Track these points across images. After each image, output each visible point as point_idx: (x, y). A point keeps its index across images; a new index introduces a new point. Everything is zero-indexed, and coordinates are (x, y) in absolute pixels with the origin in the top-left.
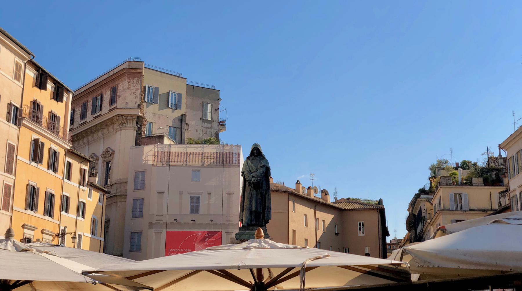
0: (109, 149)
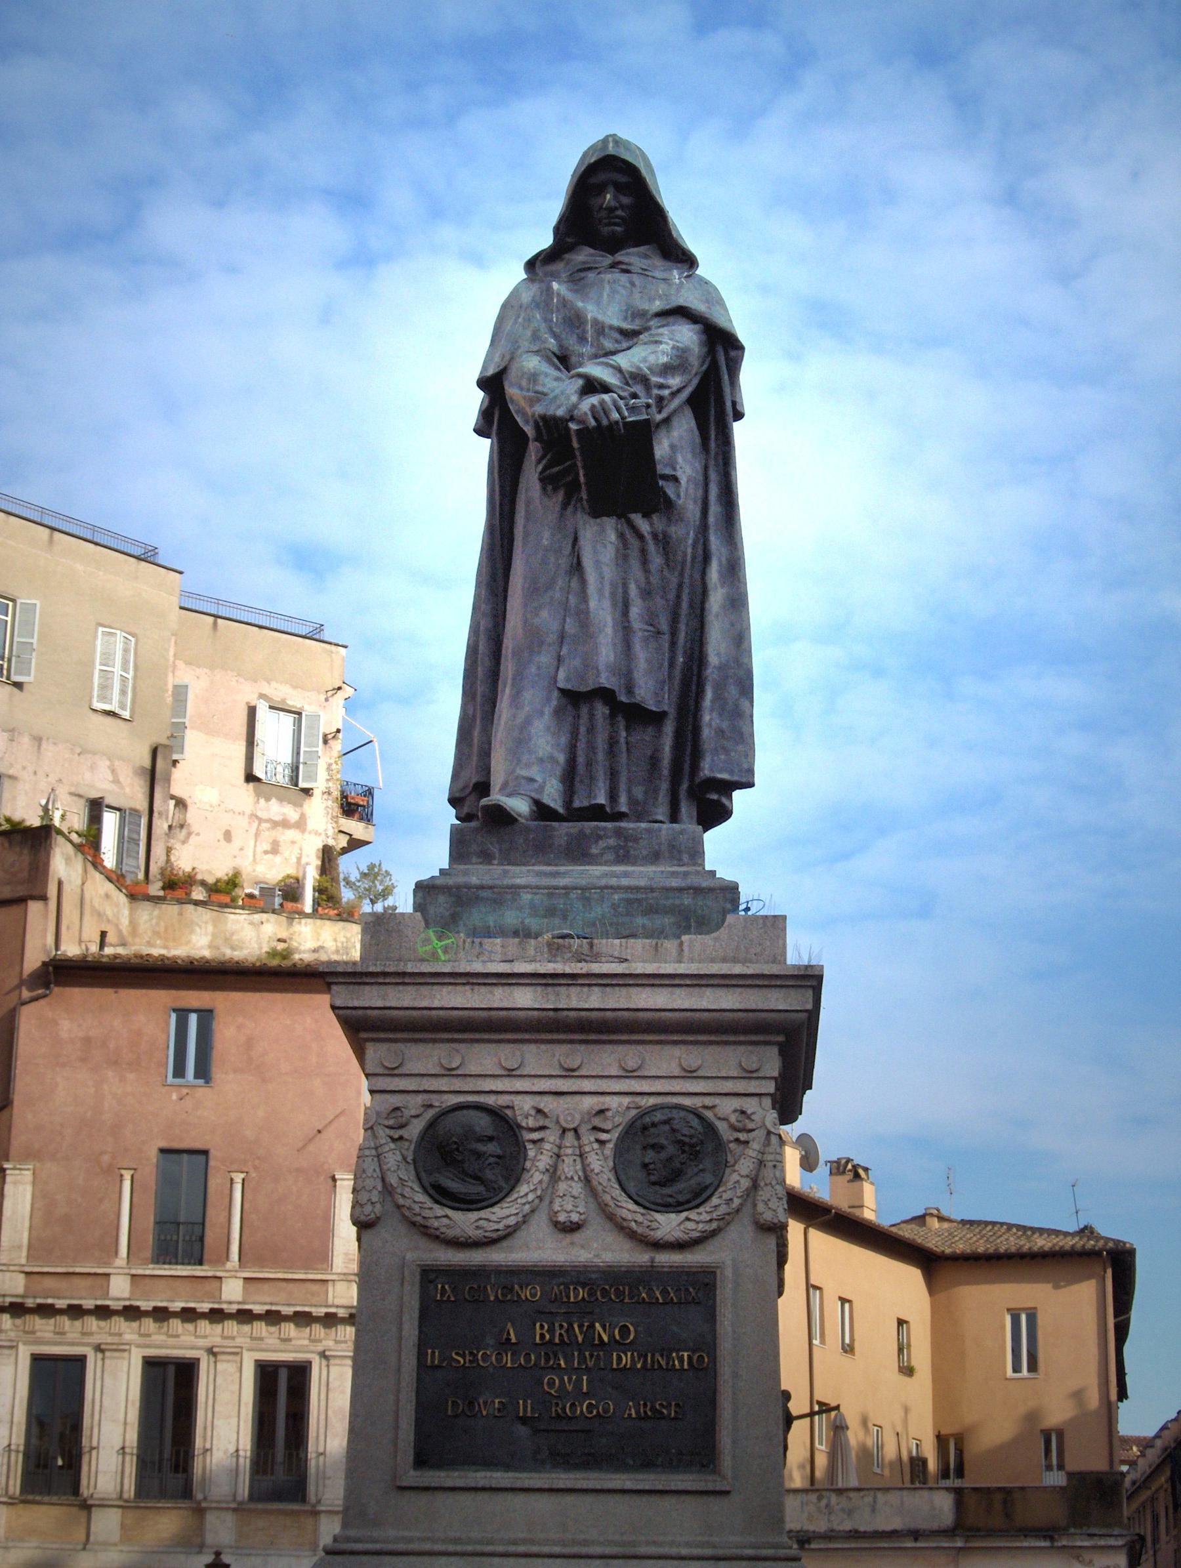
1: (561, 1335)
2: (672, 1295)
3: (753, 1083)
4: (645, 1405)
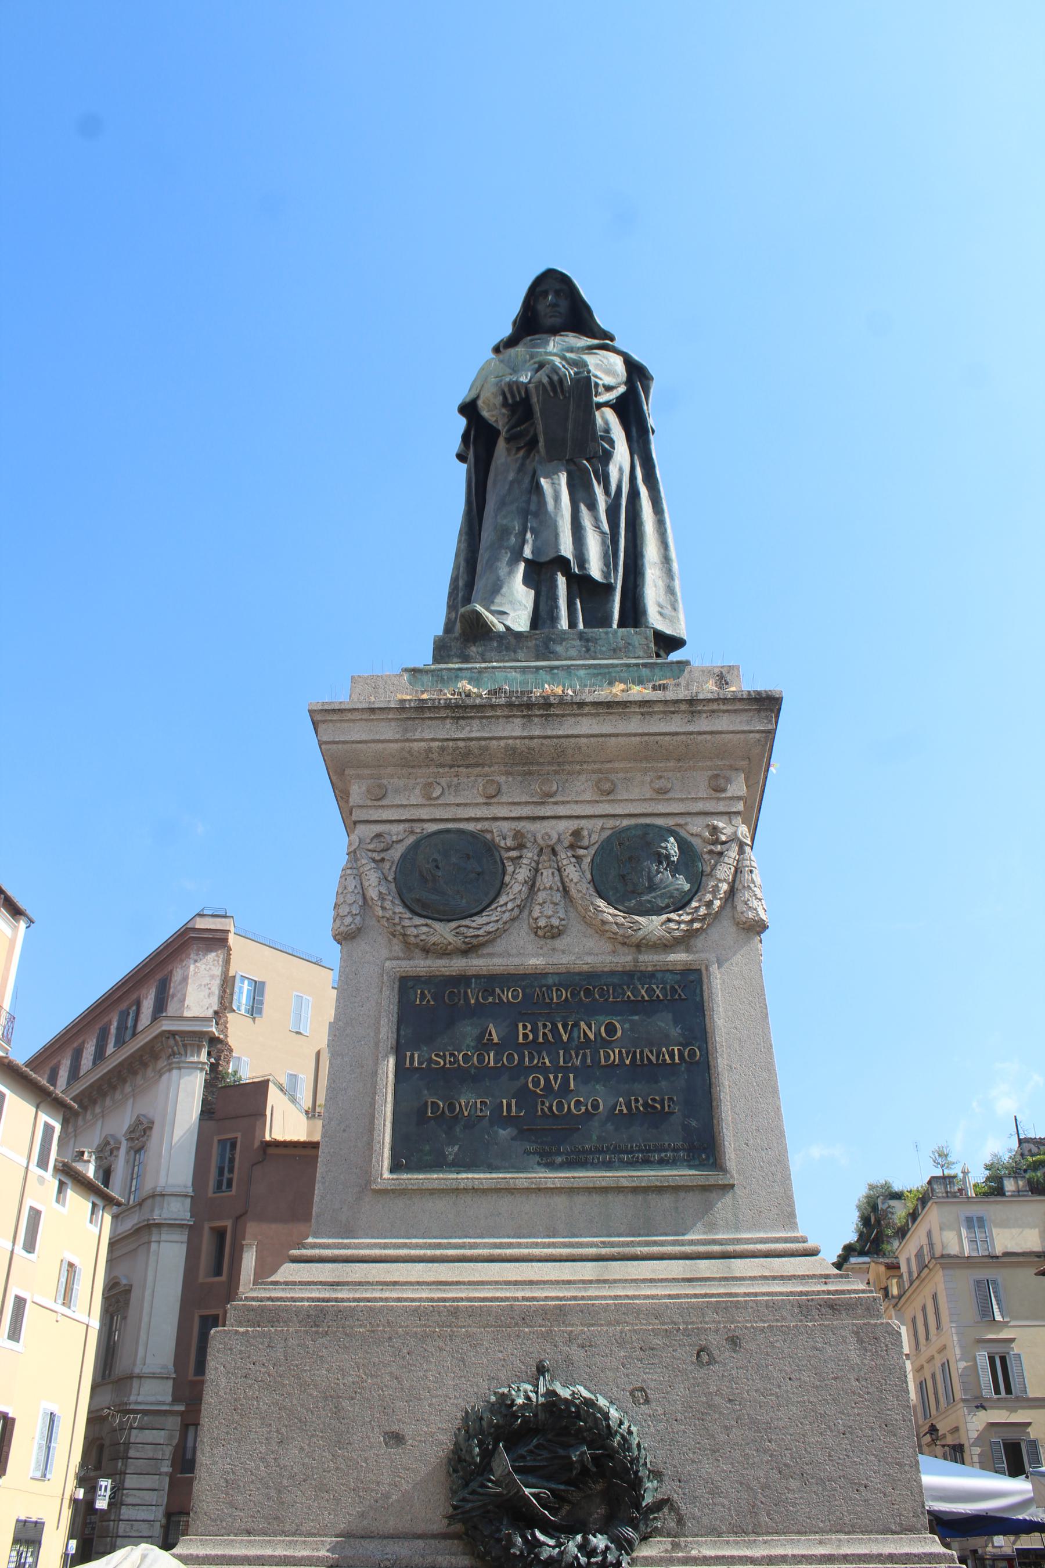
0: (142, 1118)
1: (544, 1034)
2: (658, 992)
3: (721, 803)
4: (637, 1101)
